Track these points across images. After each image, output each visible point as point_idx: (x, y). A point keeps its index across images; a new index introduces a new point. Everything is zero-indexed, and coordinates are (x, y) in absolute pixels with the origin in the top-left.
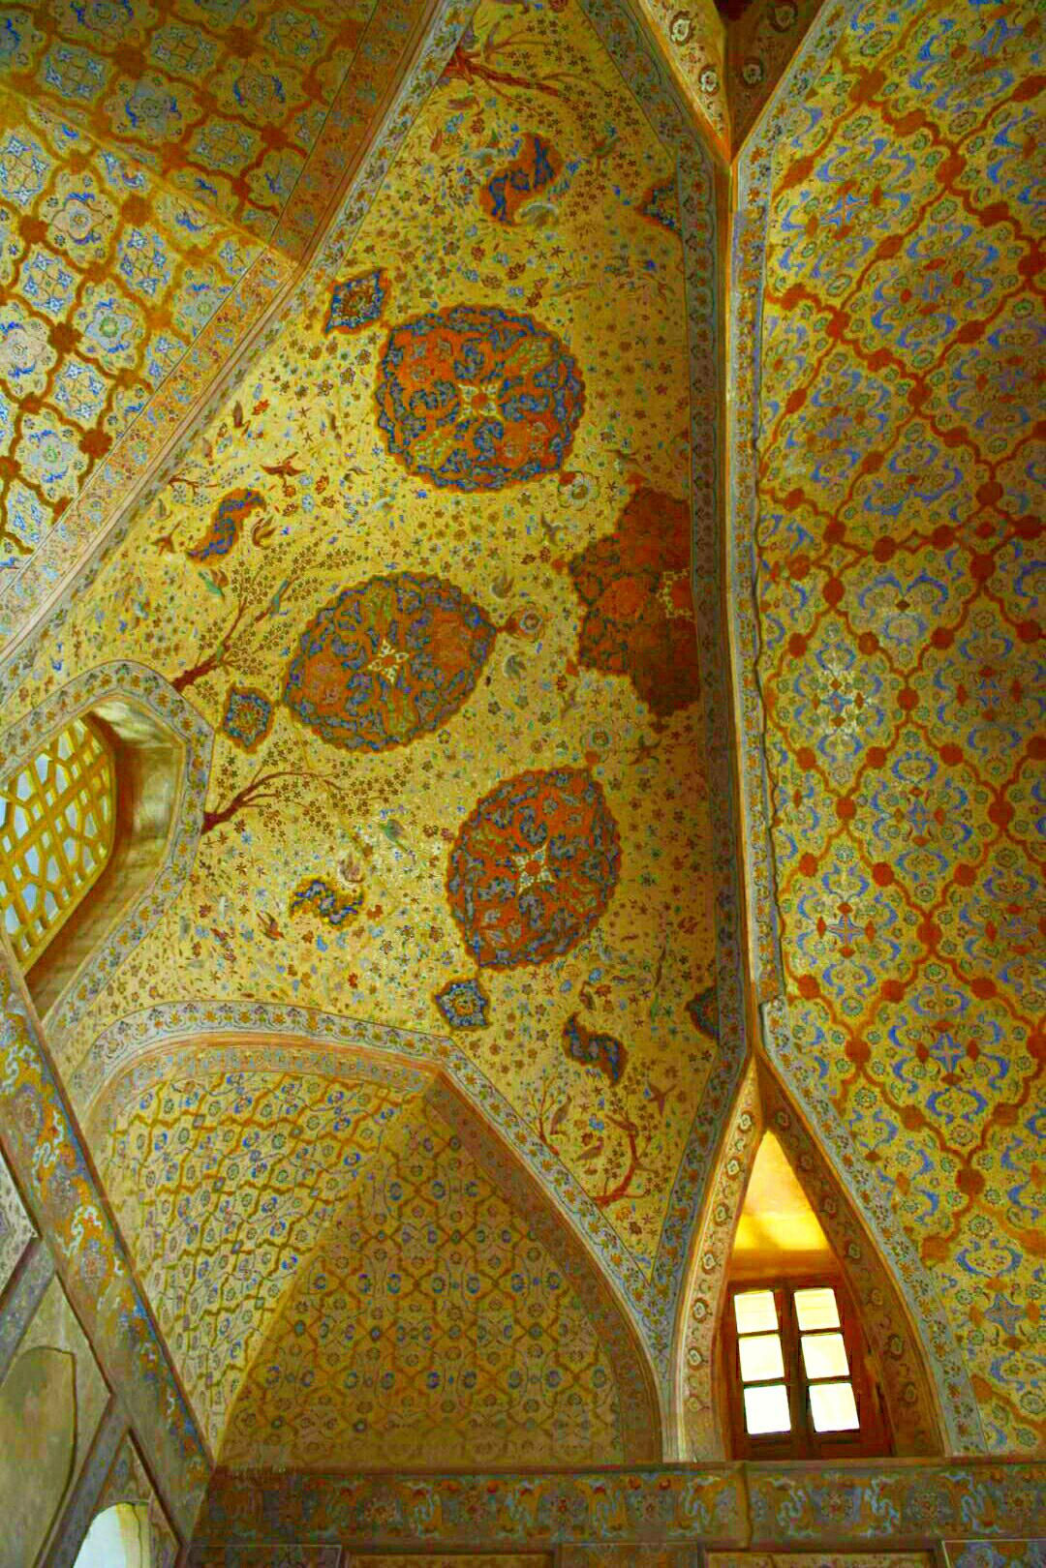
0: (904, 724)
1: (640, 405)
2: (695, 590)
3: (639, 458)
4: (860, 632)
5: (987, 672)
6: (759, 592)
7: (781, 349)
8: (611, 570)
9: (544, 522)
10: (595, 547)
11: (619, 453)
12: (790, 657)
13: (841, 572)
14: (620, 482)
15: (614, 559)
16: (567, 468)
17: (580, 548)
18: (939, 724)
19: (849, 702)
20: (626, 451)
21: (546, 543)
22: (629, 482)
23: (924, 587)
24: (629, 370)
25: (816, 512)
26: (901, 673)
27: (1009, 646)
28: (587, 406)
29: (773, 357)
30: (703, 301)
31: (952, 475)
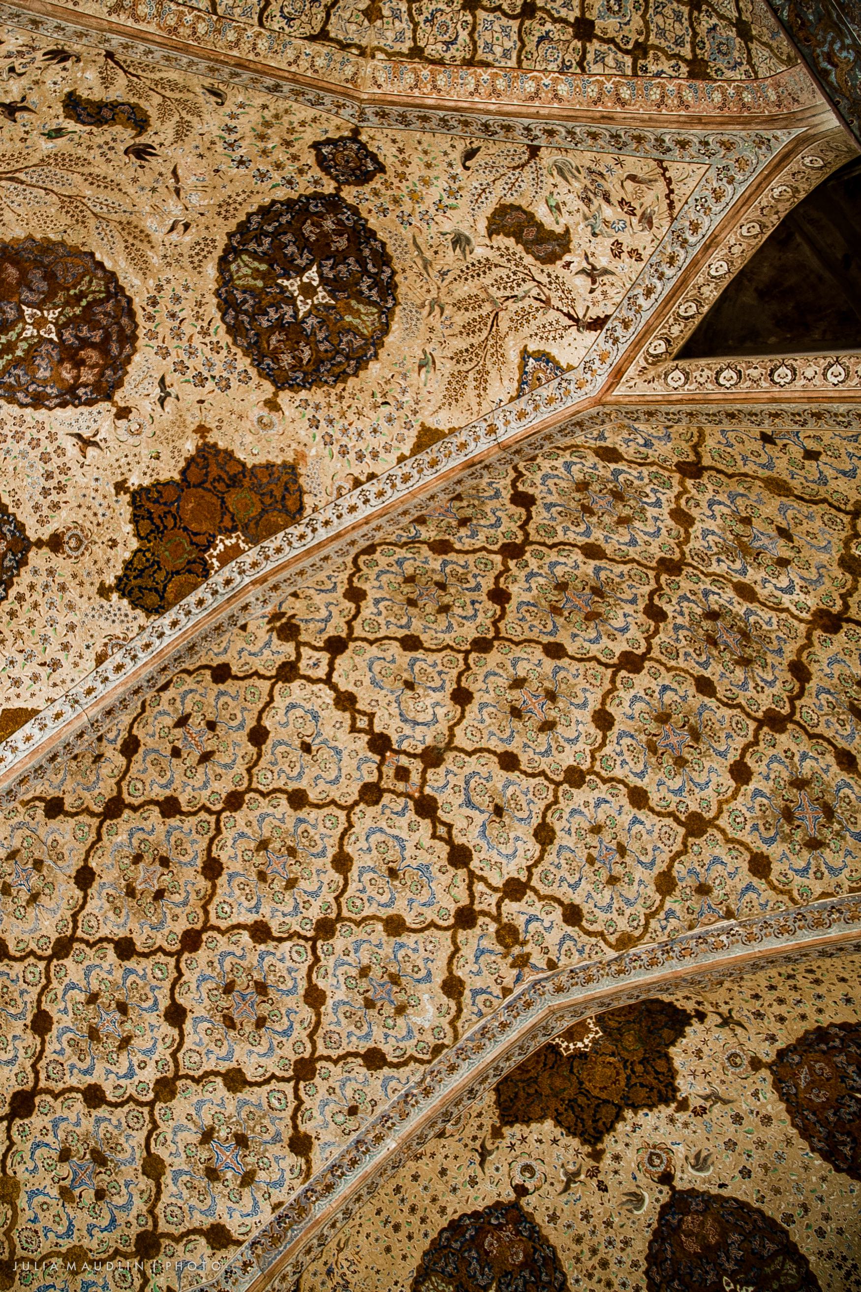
0: (597, 774)
1: (435, 1177)
2: (568, 1023)
3: (478, 1143)
4: (538, 847)
5: (516, 713)
6: (541, 975)
7: (340, 1118)
8: (581, 1100)
9: (566, 1189)
10: (568, 1129)
11: (482, 1164)
12: (584, 923)
13: (495, 890)
14: (507, 1141)
15: (572, 1104)
16: (513, 1196)
17: (575, 1142)
18: (582, 739)
19: (601, 842)
20: (478, 1158)
21: (582, 1177)
22: (502, 1136)
23: (476, 799)
24: (413, 1209)
25: (457, 950)
26: (556, 791)
27: (483, 706)
28: (456, 1216)
29: (352, 1124)
30: (333, 1226)
31: (374, 839)
